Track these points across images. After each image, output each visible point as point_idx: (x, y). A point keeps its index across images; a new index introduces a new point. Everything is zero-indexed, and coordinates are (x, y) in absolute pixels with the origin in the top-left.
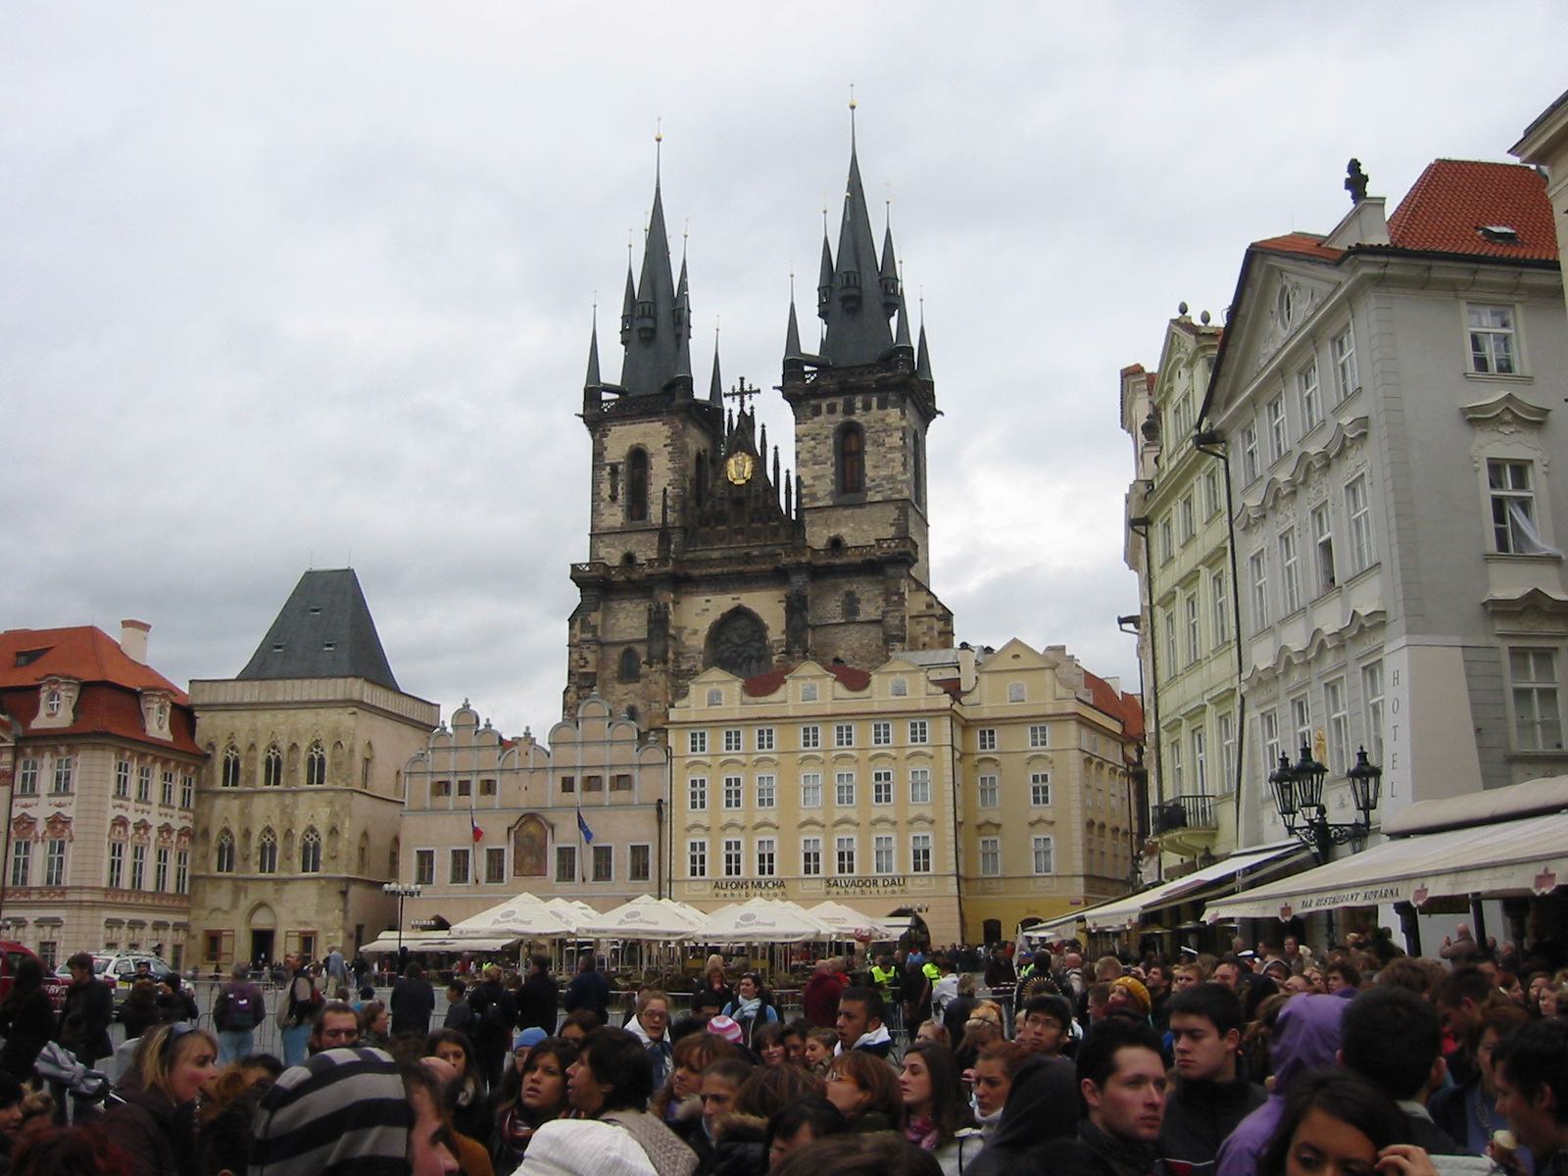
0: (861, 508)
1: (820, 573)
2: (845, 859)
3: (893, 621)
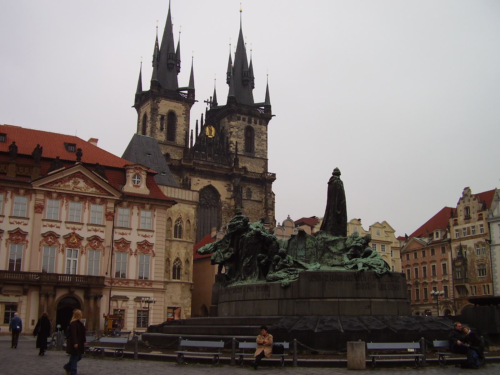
0: (253, 159)
3: (270, 202)
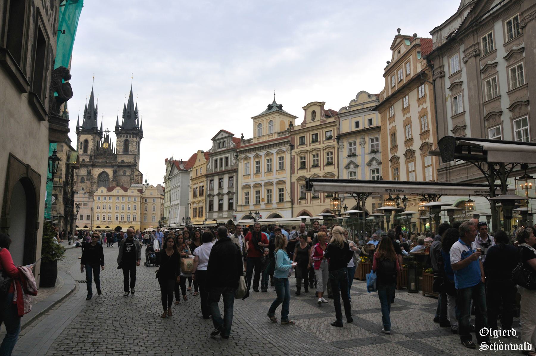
1: (119, 166)
2: (122, 218)
3: (132, 176)
